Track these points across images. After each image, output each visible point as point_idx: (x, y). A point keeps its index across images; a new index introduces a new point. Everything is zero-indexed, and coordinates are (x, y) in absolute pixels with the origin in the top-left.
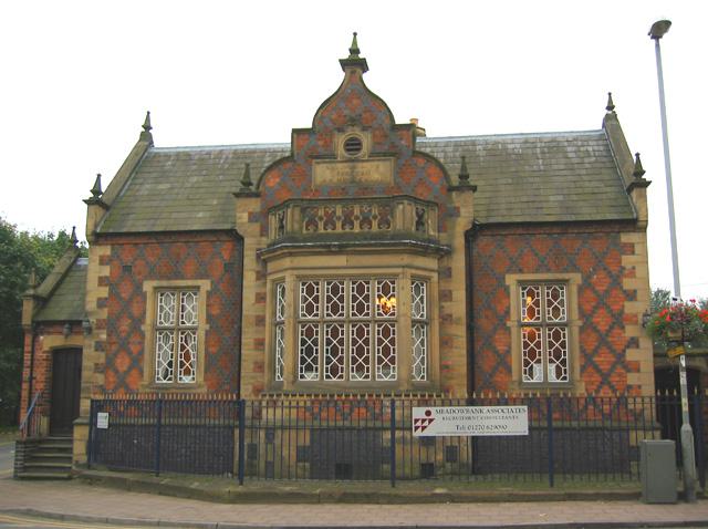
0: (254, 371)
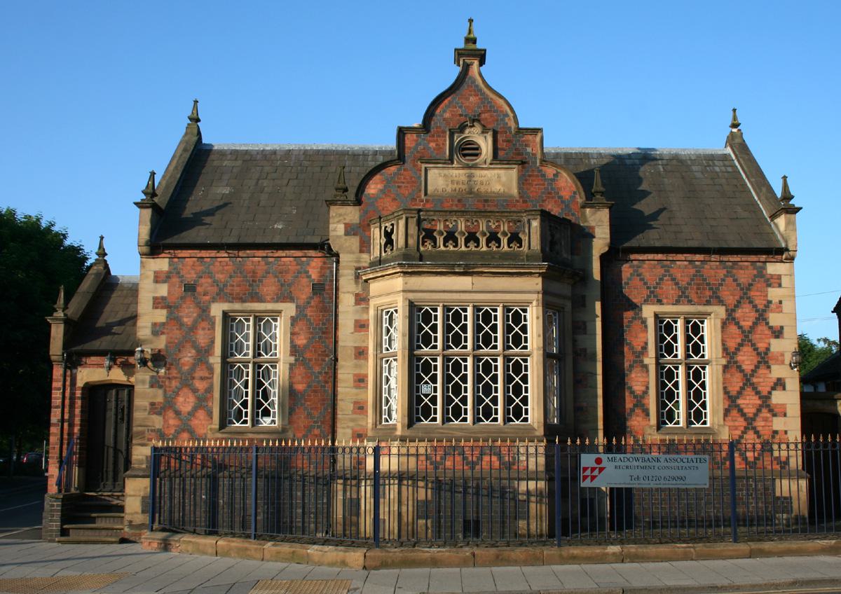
0: (354, 412)
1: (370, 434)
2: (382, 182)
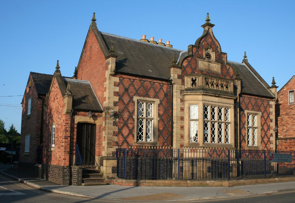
0: (180, 138)
1: (201, 145)
2: (187, 62)
